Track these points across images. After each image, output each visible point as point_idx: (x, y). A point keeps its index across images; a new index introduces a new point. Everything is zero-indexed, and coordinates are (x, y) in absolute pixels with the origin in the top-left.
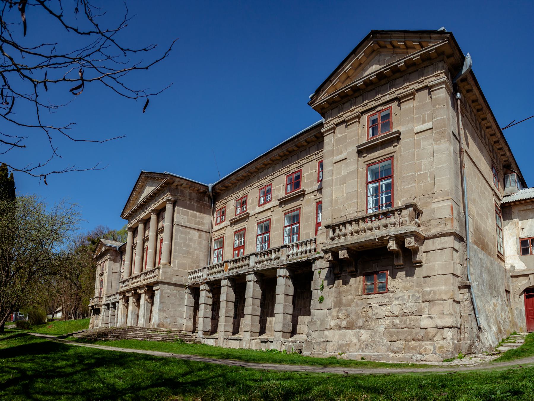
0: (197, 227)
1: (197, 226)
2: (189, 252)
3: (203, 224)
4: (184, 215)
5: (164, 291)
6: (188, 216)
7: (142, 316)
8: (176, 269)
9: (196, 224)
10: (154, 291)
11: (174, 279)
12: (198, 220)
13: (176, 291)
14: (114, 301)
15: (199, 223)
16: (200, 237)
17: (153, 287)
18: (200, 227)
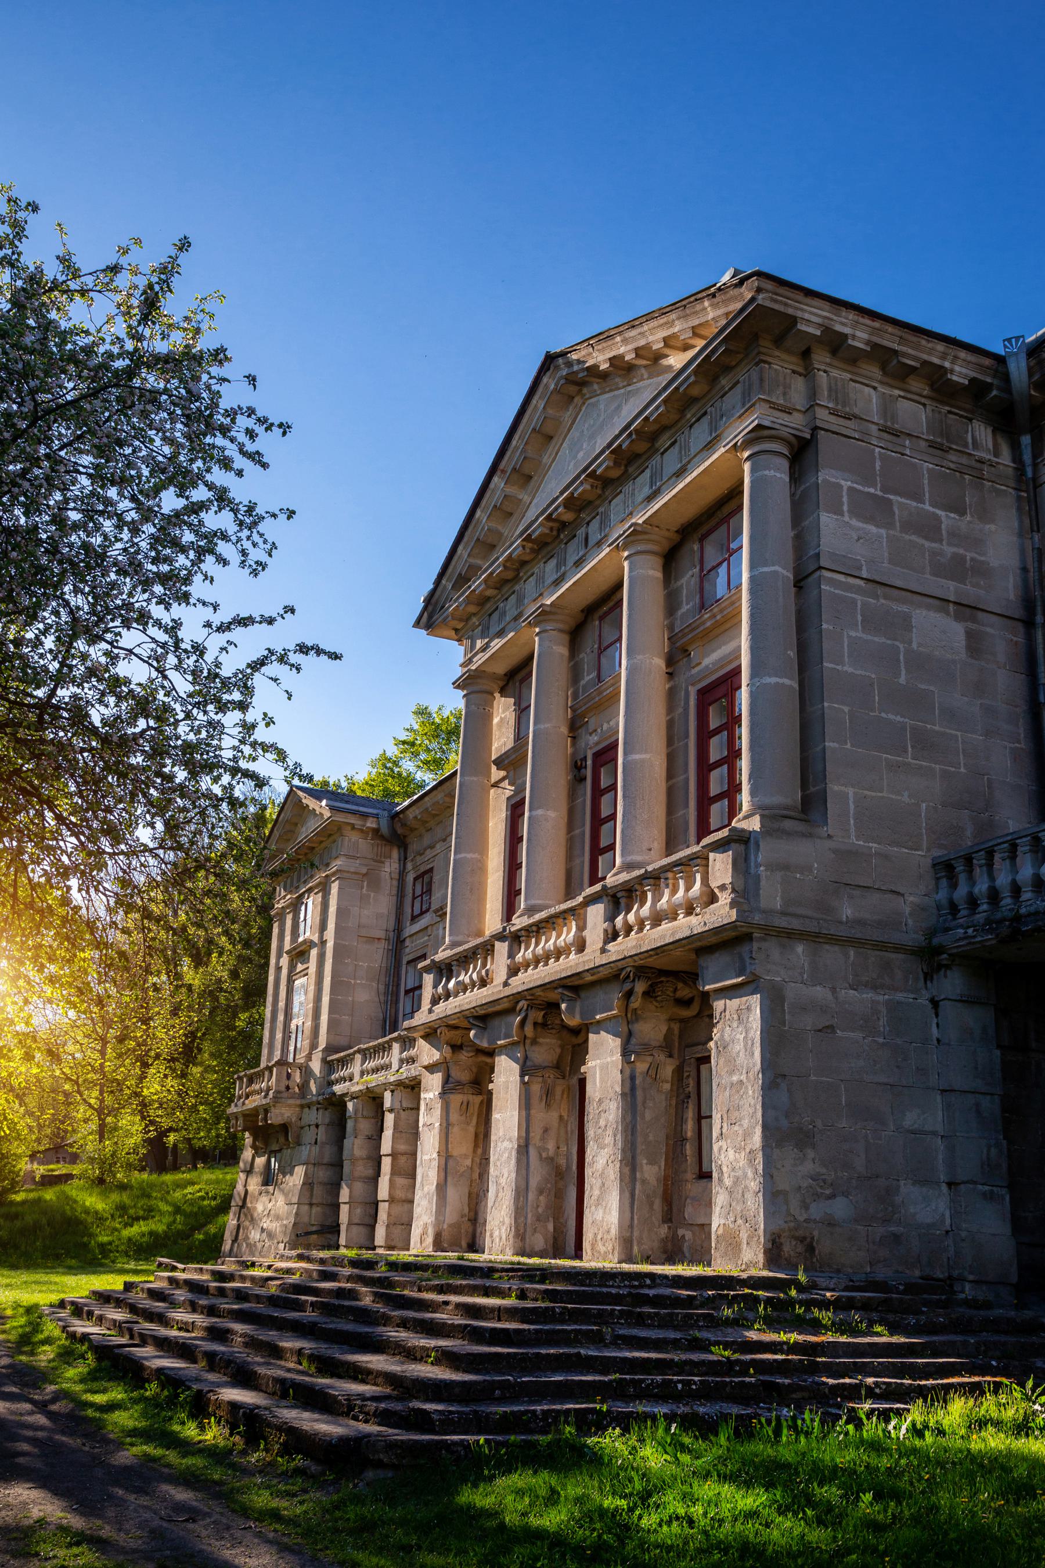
0: (950, 589)
1: (952, 585)
2: (924, 743)
3: (980, 570)
4: (870, 519)
5: (793, 992)
6: (890, 525)
7: (613, 1173)
8: (855, 841)
9: (939, 570)
10: (706, 996)
11: (847, 912)
12: (949, 550)
13: (869, 995)
14: (373, 1080)
15: (957, 569)
16: (975, 644)
17: (692, 977)
18: (970, 591)
